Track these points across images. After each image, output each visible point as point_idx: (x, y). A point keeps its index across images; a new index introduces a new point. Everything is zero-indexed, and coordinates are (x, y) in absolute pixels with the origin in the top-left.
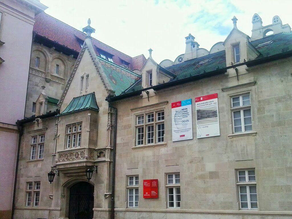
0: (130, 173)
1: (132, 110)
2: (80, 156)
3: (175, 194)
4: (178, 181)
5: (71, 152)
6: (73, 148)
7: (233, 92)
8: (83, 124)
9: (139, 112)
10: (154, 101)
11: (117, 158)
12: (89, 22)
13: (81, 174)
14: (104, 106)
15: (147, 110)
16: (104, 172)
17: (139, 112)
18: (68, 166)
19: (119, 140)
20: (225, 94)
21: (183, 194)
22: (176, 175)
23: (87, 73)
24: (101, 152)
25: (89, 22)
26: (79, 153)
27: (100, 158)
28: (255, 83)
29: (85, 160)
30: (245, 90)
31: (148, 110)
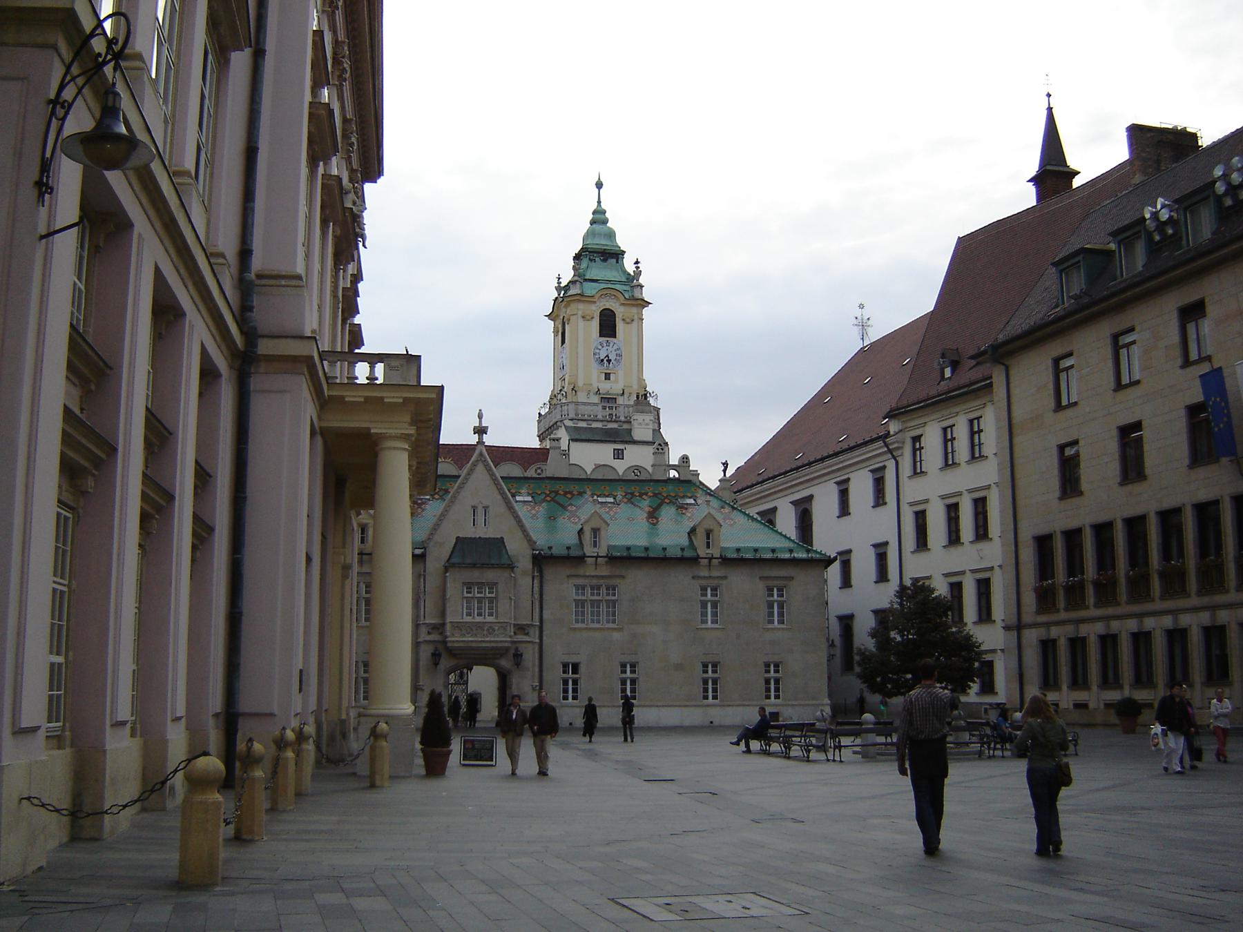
0: (567, 659)
1: (568, 576)
5: (480, 626)
6: (479, 619)
7: (704, 582)
9: (580, 581)
10: (605, 571)
11: (544, 638)
12: (480, 416)
14: (525, 563)
16: (530, 656)
17: (580, 581)
18: (474, 645)
23: (485, 503)
24: (521, 629)
25: (480, 416)
28: (725, 578)
29: (509, 639)
30: (715, 582)
31: (595, 581)
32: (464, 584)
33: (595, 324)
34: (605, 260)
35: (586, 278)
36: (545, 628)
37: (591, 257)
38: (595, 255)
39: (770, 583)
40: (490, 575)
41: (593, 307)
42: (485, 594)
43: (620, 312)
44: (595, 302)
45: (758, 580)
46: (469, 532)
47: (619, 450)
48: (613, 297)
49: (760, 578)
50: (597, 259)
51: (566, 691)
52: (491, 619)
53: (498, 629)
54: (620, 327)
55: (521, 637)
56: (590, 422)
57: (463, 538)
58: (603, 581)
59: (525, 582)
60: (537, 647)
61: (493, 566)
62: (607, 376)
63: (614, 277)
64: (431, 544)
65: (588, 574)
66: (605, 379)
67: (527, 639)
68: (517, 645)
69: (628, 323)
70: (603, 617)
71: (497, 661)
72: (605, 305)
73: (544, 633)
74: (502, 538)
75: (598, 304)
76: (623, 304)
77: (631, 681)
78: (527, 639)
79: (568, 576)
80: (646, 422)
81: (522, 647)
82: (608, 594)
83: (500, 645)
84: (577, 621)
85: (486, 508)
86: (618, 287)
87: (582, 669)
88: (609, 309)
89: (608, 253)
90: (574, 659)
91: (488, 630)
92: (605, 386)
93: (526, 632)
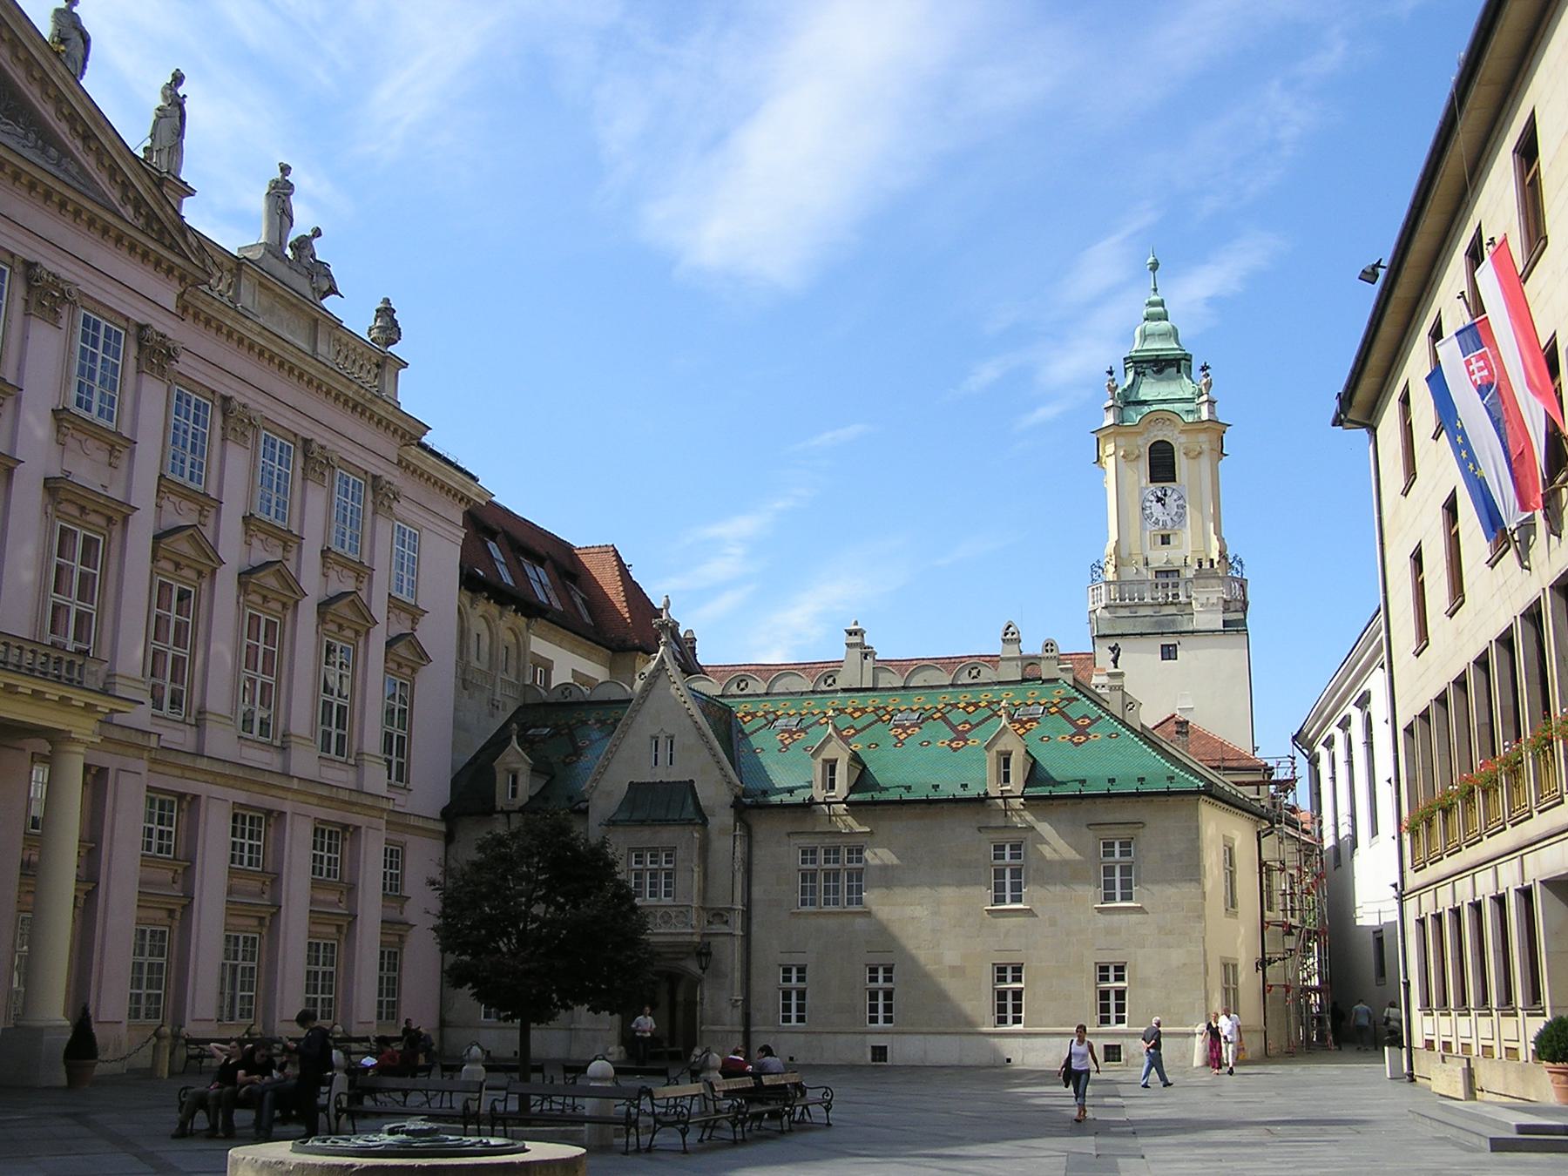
1: (789, 834)
2: (674, 921)
3: (881, 1002)
4: (888, 979)
8: (680, 854)
9: (806, 842)
11: (754, 928)
13: (670, 956)
14: (722, 819)
15: (827, 840)
16: (729, 954)
17: (806, 842)
19: (757, 892)
20: (985, 836)
21: (808, 1001)
22: (884, 969)
23: (670, 731)
24: (719, 915)
26: (673, 915)
27: (714, 927)
31: (828, 841)
32: (631, 850)
33: (1144, 466)
34: (1160, 371)
35: (1130, 400)
36: (754, 913)
37: (1139, 370)
38: (1145, 365)
39: (1109, 833)
40: (666, 836)
41: (1140, 440)
42: (661, 864)
43: (1179, 442)
44: (1140, 434)
45: (1085, 830)
46: (647, 775)
47: (1169, 646)
48: (1168, 423)
49: (1088, 825)
50: (1147, 371)
51: (787, 1008)
52: (668, 901)
53: (677, 916)
54: (1182, 464)
55: (718, 928)
56: (1133, 609)
57: (638, 783)
58: (840, 840)
59: (725, 846)
60: (738, 942)
61: (665, 822)
62: (1165, 540)
63: (1173, 393)
64: (595, 795)
65: (817, 830)
66: (1163, 544)
67: (725, 929)
68: (711, 939)
69: (1193, 458)
70: (844, 895)
71: (683, 963)
72: (1155, 436)
73: (754, 921)
74: (692, 781)
75: (1146, 436)
76: (1182, 431)
77: (798, 992)
78: (725, 929)
79: (789, 834)
80: (1211, 601)
81: (715, 941)
82: (850, 860)
83: (680, 939)
84: (804, 903)
85: (671, 739)
86: (1177, 407)
87: (809, 974)
88: (1163, 441)
89: (1164, 360)
90: (799, 959)
91: (662, 917)
92: (1160, 557)
93: (725, 919)
